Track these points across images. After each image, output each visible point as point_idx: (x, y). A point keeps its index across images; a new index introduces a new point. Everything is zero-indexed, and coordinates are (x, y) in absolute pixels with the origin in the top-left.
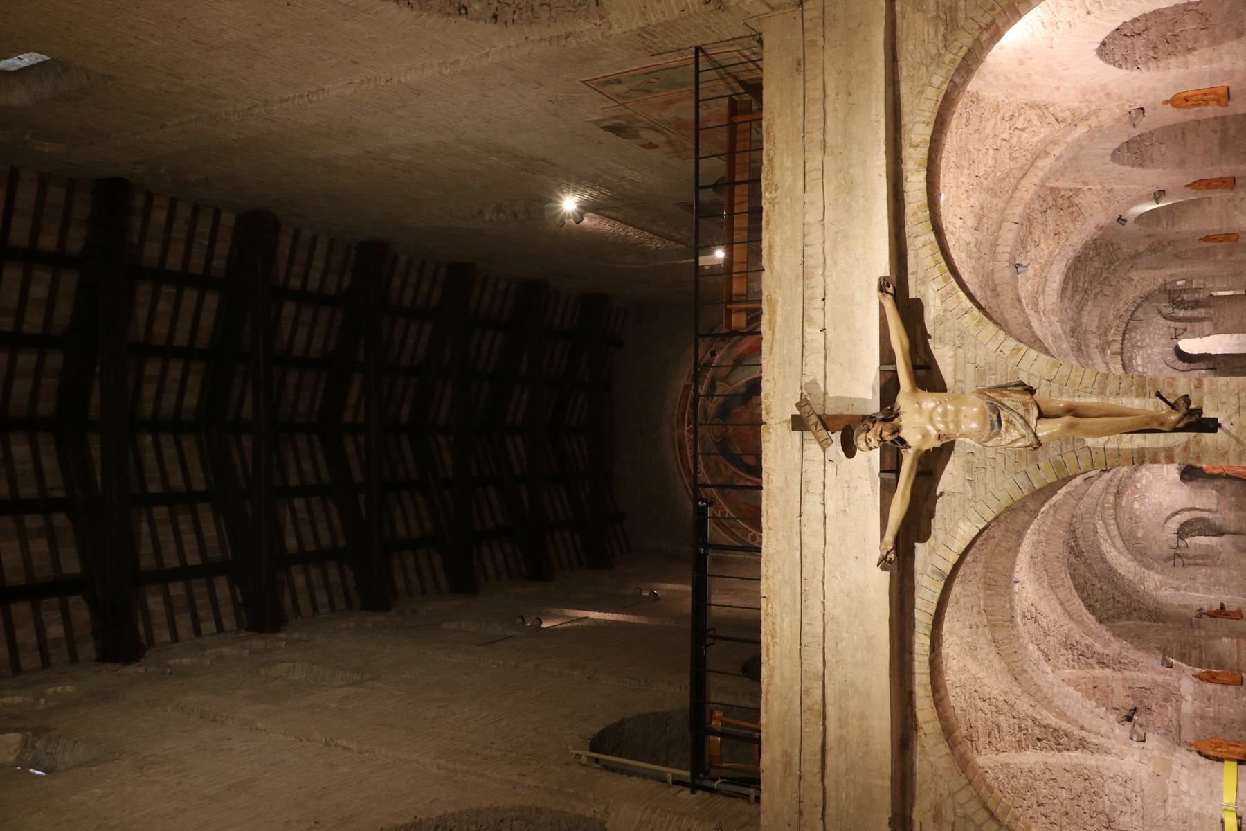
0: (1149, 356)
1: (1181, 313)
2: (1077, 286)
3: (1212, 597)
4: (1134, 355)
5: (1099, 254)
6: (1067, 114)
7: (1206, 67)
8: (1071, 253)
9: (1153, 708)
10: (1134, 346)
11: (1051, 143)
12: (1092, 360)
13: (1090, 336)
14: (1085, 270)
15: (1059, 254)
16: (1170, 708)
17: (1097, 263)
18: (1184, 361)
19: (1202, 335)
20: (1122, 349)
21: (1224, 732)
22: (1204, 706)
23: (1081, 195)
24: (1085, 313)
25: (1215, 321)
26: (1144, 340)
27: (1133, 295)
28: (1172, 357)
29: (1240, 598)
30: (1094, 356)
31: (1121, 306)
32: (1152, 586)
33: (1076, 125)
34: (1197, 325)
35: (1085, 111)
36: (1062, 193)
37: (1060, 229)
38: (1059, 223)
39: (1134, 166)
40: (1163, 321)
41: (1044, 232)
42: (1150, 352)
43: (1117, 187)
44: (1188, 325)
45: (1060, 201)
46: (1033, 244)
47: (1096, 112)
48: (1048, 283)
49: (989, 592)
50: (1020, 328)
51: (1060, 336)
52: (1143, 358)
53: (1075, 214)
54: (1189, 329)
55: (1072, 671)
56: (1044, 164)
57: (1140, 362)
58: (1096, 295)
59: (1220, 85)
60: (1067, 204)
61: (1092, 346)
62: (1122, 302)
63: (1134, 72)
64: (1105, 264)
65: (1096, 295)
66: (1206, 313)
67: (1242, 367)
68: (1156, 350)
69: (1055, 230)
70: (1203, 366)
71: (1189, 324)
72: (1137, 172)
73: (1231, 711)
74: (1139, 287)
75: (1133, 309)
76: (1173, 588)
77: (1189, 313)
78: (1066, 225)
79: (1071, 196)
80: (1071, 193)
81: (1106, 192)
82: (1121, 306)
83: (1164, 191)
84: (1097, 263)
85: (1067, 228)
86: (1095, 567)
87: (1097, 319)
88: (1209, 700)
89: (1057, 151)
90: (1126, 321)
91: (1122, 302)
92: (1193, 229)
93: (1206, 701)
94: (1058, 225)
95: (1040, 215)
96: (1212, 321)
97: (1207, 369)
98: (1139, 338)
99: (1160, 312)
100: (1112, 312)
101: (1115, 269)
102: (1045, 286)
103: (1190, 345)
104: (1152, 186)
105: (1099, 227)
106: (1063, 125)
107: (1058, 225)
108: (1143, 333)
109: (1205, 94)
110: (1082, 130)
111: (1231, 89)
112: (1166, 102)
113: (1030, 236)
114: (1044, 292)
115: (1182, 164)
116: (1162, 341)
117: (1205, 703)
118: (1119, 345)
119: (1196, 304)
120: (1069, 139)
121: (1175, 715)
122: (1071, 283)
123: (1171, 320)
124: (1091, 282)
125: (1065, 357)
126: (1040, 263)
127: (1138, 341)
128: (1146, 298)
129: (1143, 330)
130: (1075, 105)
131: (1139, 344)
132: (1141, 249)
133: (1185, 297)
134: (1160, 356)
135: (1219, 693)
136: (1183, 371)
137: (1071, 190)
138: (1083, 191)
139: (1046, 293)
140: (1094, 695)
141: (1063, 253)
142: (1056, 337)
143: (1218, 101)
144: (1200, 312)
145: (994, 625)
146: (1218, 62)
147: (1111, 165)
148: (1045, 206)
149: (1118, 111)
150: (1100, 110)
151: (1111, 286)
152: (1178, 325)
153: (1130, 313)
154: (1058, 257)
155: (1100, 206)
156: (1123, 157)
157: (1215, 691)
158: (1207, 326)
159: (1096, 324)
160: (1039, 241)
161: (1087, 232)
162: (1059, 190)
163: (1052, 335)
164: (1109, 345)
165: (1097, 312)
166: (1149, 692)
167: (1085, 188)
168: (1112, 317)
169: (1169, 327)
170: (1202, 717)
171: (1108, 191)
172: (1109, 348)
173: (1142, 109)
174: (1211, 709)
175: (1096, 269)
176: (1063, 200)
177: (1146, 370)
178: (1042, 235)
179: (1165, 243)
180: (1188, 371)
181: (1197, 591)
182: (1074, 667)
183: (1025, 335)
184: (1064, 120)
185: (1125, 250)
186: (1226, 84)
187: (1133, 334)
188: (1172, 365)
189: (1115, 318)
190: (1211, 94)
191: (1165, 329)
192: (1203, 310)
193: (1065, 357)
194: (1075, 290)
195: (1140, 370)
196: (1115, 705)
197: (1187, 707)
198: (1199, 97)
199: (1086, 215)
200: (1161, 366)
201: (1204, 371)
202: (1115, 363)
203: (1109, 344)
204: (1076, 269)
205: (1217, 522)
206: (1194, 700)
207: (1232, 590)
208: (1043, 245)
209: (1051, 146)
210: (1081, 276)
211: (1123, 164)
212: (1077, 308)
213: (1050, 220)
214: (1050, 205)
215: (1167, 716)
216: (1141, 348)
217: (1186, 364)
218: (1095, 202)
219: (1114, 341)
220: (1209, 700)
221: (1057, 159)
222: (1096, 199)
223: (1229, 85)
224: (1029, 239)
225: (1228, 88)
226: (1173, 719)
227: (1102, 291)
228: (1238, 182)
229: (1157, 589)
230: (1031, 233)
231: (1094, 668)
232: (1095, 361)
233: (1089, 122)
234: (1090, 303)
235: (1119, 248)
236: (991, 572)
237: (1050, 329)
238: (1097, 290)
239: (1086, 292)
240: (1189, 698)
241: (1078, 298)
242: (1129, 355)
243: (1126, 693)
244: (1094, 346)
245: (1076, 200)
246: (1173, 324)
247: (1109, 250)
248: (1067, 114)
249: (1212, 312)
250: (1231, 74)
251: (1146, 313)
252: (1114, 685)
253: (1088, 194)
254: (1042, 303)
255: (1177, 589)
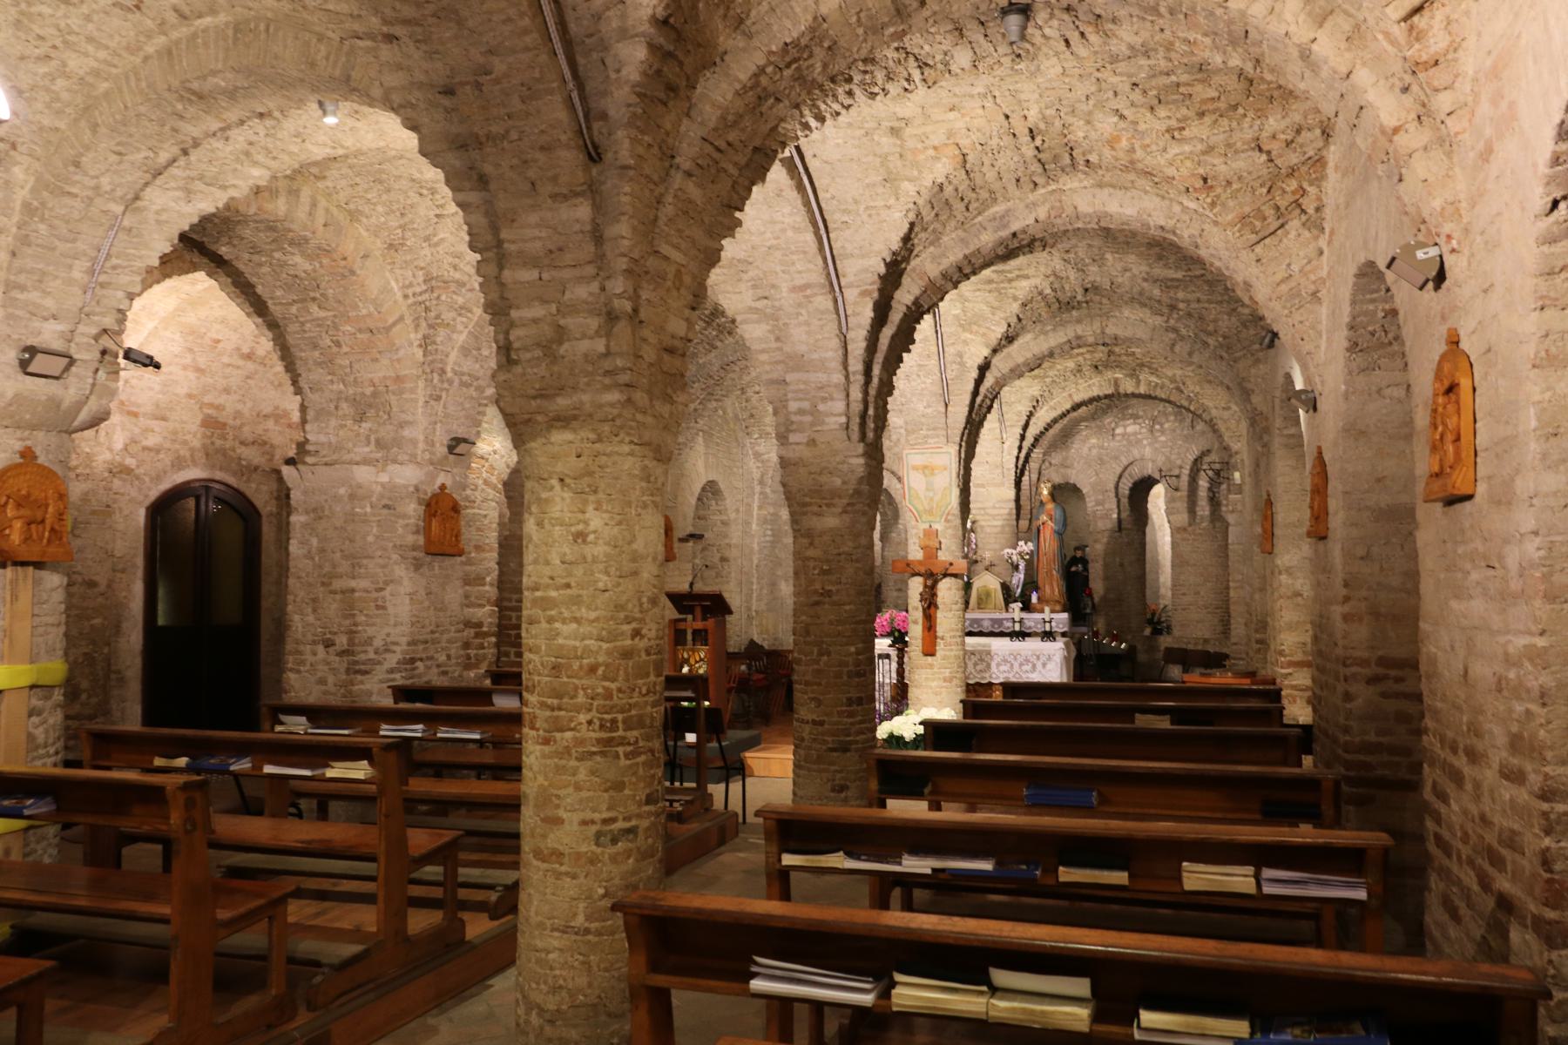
0: (1139, 442)
1: (1203, 483)
2: (1177, 287)
3: (754, 526)
4: (1140, 421)
5: (1244, 325)
6: (1437, 42)
7: (1530, 420)
8: (1186, 234)
9: (364, 425)
10: (1154, 420)
11: (1357, 27)
12: (1054, 330)
13: (1097, 325)
14: (1209, 302)
15: (1185, 209)
16: (367, 449)
17: (1226, 324)
18: (1132, 490)
19: (1169, 512)
20: (1126, 395)
21: (336, 528)
22: (374, 499)
23: (1307, 234)
24: (1144, 314)
25: (1190, 529)
26: (1163, 432)
27: (1211, 404)
28: (1137, 472)
29: (755, 562)
30: (1062, 334)
31: (1191, 388)
32: (761, 449)
33: (1405, 90)
34: (1182, 506)
35: (1444, 102)
36: (1312, 190)
37: (1219, 190)
38: (1235, 186)
39: (1352, 328)
40: (1191, 457)
41: (1210, 150)
42: (1145, 442)
43: (1324, 311)
44: (1184, 493)
45: (1293, 185)
46: (1174, 123)
47: (1446, 143)
48: (1120, 193)
49: (230, 32)
50: (805, 9)
51: (1005, 226)
52: (1135, 434)
53: (1258, 224)
54: (1179, 494)
55: (399, 296)
56: (1288, 17)
57: (1130, 429)
58: (1175, 330)
59: (1481, 472)
60: (1283, 203)
61: (1079, 330)
62: (1197, 389)
63: (1540, 190)
64: (1225, 337)
65: (1175, 330)
66: (1202, 517)
67: (1122, 565)
68: (1148, 452)
69: (1215, 178)
70: (1124, 515)
71: (1185, 493)
72: (1341, 339)
73: (370, 539)
74: (1226, 414)
75: (1192, 408)
76: (762, 476)
77: (1203, 493)
78: (1231, 203)
79: (1304, 211)
80: (1311, 211)
81: (1312, 288)
82: (1191, 388)
83: (1315, 409)
84: (1226, 324)
85: (1223, 205)
86: (713, 355)
87: (1128, 333)
88: (386, 506)
89: (1327, 47)
90: (1172, 399)
91: (1197, 389)
92: (1279, 480)
93: (385, 501)
94: (1229, 183)
95: (1249, 134)
96: (1190, 525)
97: (1120, 521)
98: (1166, 426)
99: (1204, 454)
100: (1179, 372)
101: (1221, 357)
102: (1113, 186)
103: (1158, 498)
104: (1323, 382)
105: (1248, 285)
106: (1399, 31)
107: (1229, 183)
108: (1174, 431)
109: (1458, 439)
110: (1387, 107)
111: (1467, 505)
112: (1454, 341)
113: (1191, 114)
114: (1100, 186)
115: (1354, 431)
116: (1160, 460)
117: (378, 500)
118: (1130, 390)
119: (1214, 501)
120: (1363, 76)
121: (358, 459)
122: (1179, 275)
123: (1191, 470)
124: (1190, 315)
125: (962, 240)
126: (1132, 150)
127: (1162, 425)
128: (1212, 425)
129: (1178, 432)
130: (1469, 62)
131: (1157, 427)
132: (1256, 399)
133: (1224, 487)
134: (1138, 456)
135: (401, 522)
136: (1117, 487)
137: (1318, 210)
138: (1316, 238)
139: (1097, 191)
140: (360, 331)
141: (1186, 218)
142: (1003, 219)
143: (1437, 475)
144: (1203, 508)
145: (169, 52)
146: (1544, 456)
147: (1352, 269)
148: (1275, 147)
149: (1437, 203)
150: (1449, 155)
151: (1190, 354)
152: (1185, 479)
153: (1185, 403)
154: (1177, 208)
155: (1278, 277)
156: (1373, 301)
157: (404, 516)
158: (1183, 518)
159: (1120, 332)
160: (1183, 140)
161: (1232, 265)
162: (1318, 181)
163: (1008, 211)
164: (1131, 376)
165: (1142, 333)
166: (386, 417)
167: (1323, 243)
168: (1170, 373)
169: (1181, 467)
170: (352, 497)
171: (1314, 294)
172: (1126, 375)
173: (1441, 278)
174: (368, 510)
175: (1215, 321)
176: (1293, 193)
177: (1118, 438)
178: (1200, 147)
179: (1266, 438)
180: (1117, 495)
181: (760, 508)
182: (406, 297)
183: (788, 24)
184: (1416, 35)
185: (1253, 371)
186: (1481, 489)
187: (1172, 418)
188: (1126, 474)
189: (1173, 380)
190: (1457, 453)
191: (1179, 462)
192: (1207, 513)
193: (962, 240)
194: (1167, 284)
195: (1119, 431)
196: (356, 366)
197: (363, 474)
198: (1452, 422)
199: (1258, 249)
200: (1123, 458)
201: (1115, 516)
202: (1101, 386)
203: (1133, 374)
204: (1210, 283)
205: (894, 535)
206: (383, 485)
207: (766, 552)
208: (1174, 150)
209: (1347, 27)
210: (1198, 295)
211: (1353, 303)
212: (1141, 294)
213: (1240, 164)
214: (1279, 162)
215: (354, 446)
216: (1151, 431)
217: (1127, 492)
218: (1289, 265)
219: (1138, 382)
220: (386, 506)
221: (1305, 55)
222: (1295, 268)
223: (1477, 498)
224: (1184, 111)
225: (1470, 497)
226: (352, 455)
227: (1182, 338)
228: (1321, 545)
229: (757, 455)
230: (1201, 114)
231: (416, 331)
232: (1051, 334)
233: (1412, 127)
234: (1159, 320)
235: (1258, 361)
236: (267, 30)
237: (1022, 206)
238: (1184, 332)
239: (1173, 307)
240: (384, 478)
241: (1156, 292)
242: (1141, 413)
243: (376, 381)
244: (1080, 332)
245: (1294, 224)
246: (1186, 472)
247: (1253, 343)
248: (1437, 42)
249: (1204, 525)
250: (1504, 499)
251: (1203, 433)
252: (385, 362)
253: (1311, 250)
254: (1076, 184)
255: (761, 482)
